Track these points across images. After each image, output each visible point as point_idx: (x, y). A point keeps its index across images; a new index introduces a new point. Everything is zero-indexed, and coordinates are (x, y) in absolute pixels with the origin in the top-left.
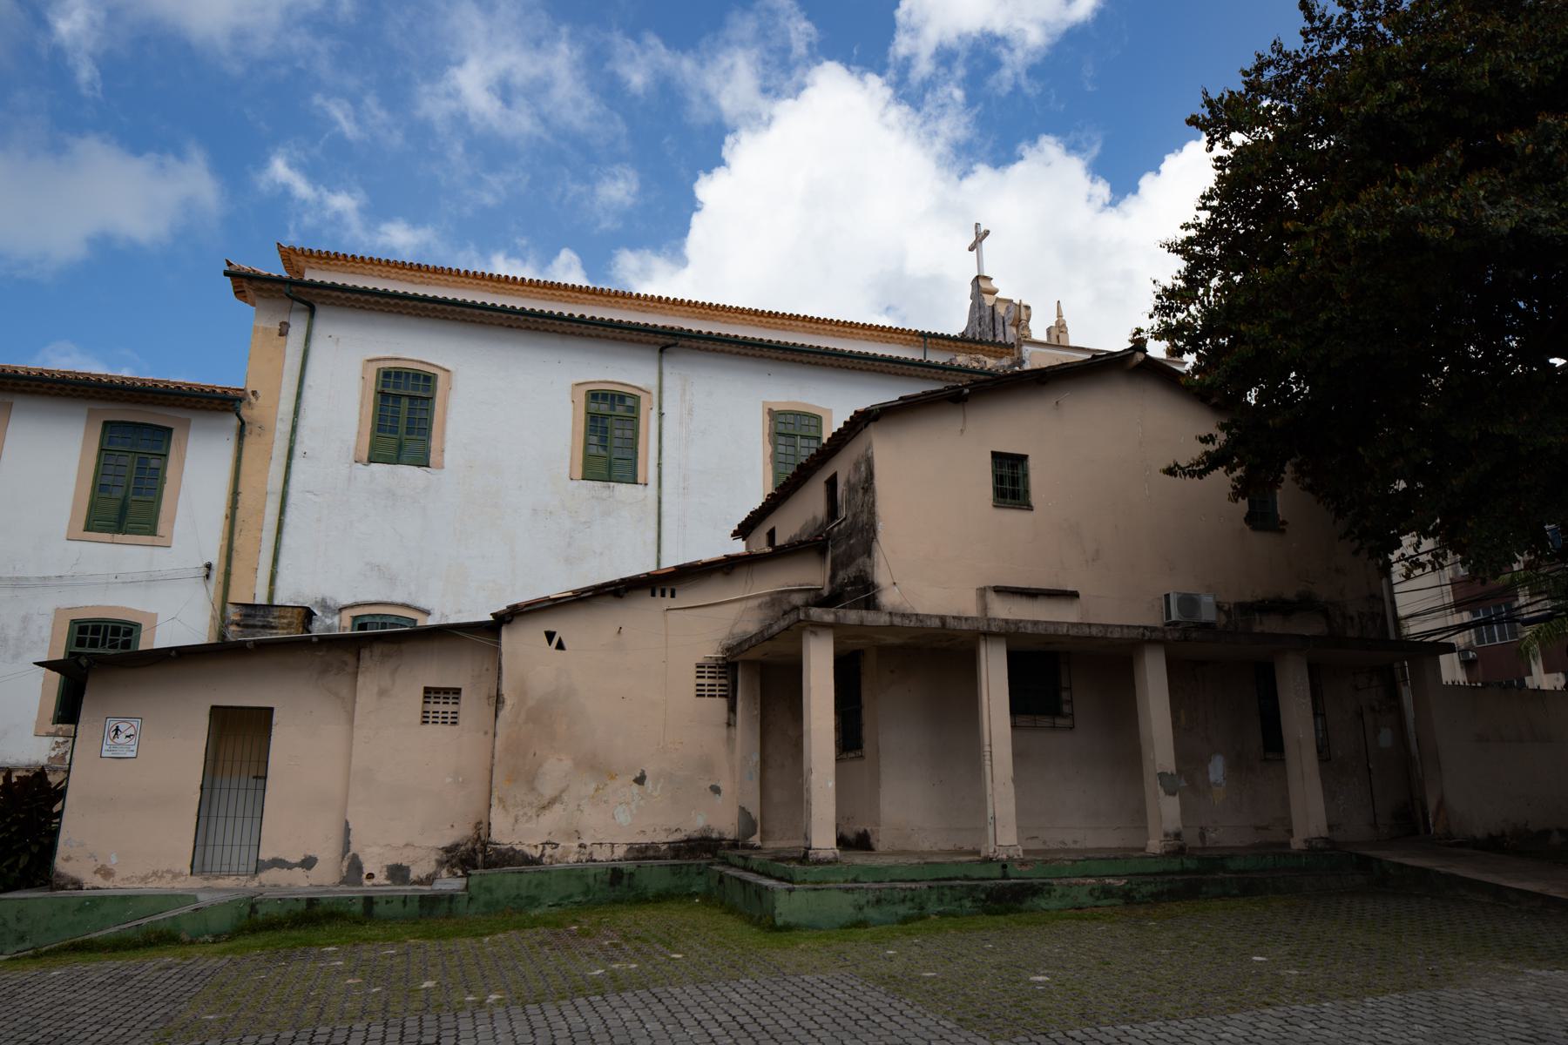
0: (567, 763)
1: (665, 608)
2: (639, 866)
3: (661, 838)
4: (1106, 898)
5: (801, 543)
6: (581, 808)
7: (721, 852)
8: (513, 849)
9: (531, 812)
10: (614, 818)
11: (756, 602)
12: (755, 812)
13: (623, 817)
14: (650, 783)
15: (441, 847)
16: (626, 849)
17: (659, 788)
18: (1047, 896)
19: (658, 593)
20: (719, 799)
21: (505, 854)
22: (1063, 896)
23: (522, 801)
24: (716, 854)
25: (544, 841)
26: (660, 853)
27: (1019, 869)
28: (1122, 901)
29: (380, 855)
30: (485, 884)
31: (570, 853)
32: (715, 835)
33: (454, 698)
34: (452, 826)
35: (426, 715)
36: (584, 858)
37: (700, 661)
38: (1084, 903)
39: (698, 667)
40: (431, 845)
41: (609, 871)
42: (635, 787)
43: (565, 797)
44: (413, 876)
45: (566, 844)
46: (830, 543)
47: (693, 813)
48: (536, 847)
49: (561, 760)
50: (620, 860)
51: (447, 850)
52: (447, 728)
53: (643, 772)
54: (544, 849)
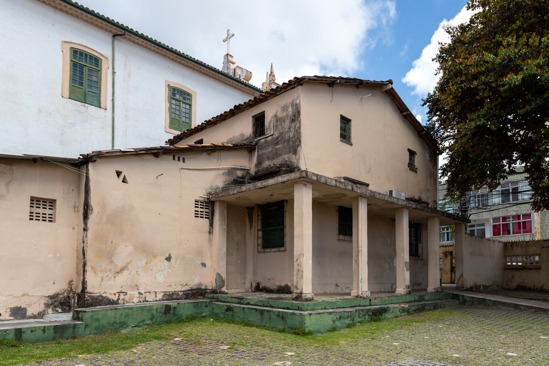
0: (130, 248)
1: (181, 168)
2: (178, 304)
3: (179, 289)
5: (245, 144)
6: (138, 273)
7: (206, 295)
8: (101, 296)
9: (111, 275)
10: (156, 278)
11: (221, 172)
12: (224, 276)
13: (160, 278)
14: (174, 260)
15: (47, 295)
16: (163, 295)
17: (177, 263)
19: (176, 158)
20: (205, 270)
21: (97, 299)
22: (393, 312)
23: (106, 269)
24: (205, 296)
25: (119, 291)
26: (179, 297)
28: (407, 313)
29: (5, 301)
30: (95, 317)
31: (134, 297)
32: (203, 287)
33: (49, 205)
34: (54, 283)
35: (32, 214)
36: (141, 300)
37: (197, 199)
39: (196, 202)
40: (41, 295)
41: (164, 307)
42: (166, 262)
43: (130, 267)
44: (29, 313)
45: (131, 293)
46: (257, 147)
47: (193, 276)
48: (115, 294)
49: (127, 246)
50: (160, 301)
51: (51, 297)
52: (47, 223)
53: (170, 254)
54: (119, 295)
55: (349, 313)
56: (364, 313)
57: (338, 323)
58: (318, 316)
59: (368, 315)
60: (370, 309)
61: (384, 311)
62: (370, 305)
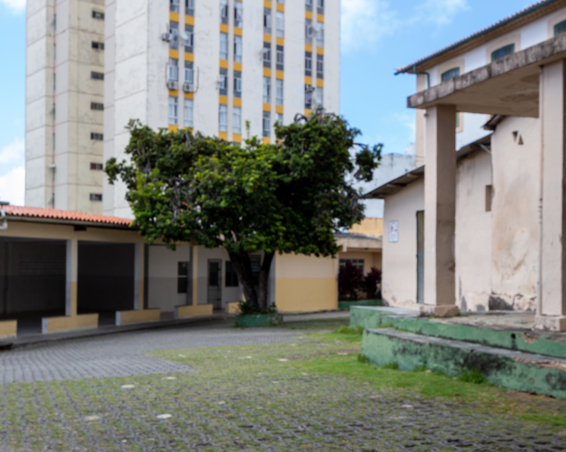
4: (562, 389)
18: (508, 372)
22: (522, 375)
27: (526, 341)
38: (539, 389)
55: (418, 347)
56: (446, 355)
57: (400, 359)
58: (376, 337)
59: (453, 361)
60: (458, 349)
61: (495, 364)
62: (514, 348)
